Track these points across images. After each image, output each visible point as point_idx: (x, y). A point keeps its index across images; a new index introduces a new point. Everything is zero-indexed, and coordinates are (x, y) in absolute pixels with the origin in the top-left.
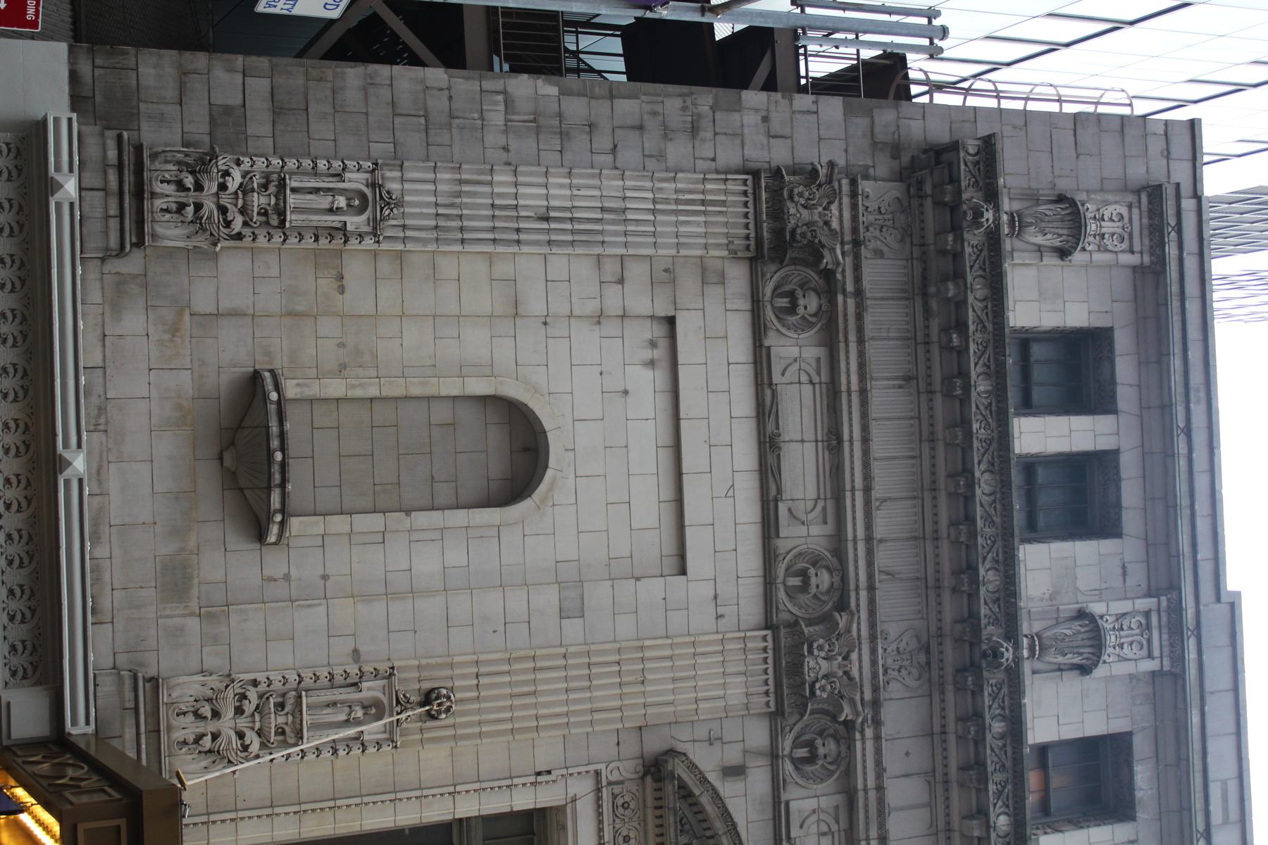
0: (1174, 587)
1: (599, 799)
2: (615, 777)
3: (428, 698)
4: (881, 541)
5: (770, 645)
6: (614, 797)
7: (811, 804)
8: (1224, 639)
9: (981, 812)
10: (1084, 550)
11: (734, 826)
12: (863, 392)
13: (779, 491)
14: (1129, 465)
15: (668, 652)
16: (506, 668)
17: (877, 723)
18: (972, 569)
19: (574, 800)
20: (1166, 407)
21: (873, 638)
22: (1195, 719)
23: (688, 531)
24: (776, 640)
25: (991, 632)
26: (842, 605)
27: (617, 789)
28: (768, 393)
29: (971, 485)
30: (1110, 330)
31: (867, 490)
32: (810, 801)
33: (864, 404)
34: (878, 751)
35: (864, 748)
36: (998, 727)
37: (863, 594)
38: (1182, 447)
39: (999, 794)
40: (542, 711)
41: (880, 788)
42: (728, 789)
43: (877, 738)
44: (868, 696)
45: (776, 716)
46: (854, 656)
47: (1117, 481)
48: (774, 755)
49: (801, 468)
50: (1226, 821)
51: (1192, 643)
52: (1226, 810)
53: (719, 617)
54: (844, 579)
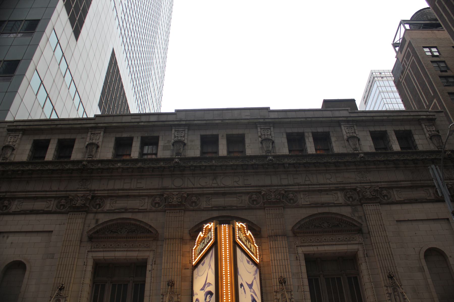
0: (88, 128)
1: (94, 251)
2: (90, 248)
3: (60, 289)
4: (58, 189)
5: (72, 213)
6: (94, 248)
7: (108, 205)
8: (103, 118)
9: (117, 169)
10: (76, 146)
11: (105, 222)
12: (26, 192)
13: (42, 210)
14: (62, 137)
15: (67, 235)
16: (58, 271)
17: (94, 190)
18: (67, 170)
19: (92, 257)
20: (52, 129)
21: (77, 191)
22: (115, 124)
23: (44, 230)
24: (71, 212)
25: (80, 166)
26: (68, 197)
27: (93, 247)
28: (22, 212)
29: (50, 170)
30: (34, 140)
31: (46, 191)
32: (108, 206)
33: (29, 192)
34: (100, 190)
35: (99, 193)
36: (100, 165)
37: (68, 193)
38: (60, 126)
39: (113, 165)
40: (70, 263)
41: (108, 190)
42: (100, 222)
43: (98, 190)
44: (89, 192)
45: (88, 212)
46: (79, 195)
47: (65, 139)
48: (96, 213)
49: (39, 205)
50: (140, 118)
51: (99, 125)
52: (137, 118)
53: (64, 224)
54: (64, 197)
